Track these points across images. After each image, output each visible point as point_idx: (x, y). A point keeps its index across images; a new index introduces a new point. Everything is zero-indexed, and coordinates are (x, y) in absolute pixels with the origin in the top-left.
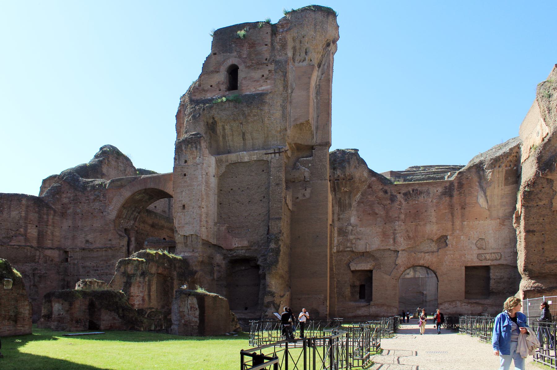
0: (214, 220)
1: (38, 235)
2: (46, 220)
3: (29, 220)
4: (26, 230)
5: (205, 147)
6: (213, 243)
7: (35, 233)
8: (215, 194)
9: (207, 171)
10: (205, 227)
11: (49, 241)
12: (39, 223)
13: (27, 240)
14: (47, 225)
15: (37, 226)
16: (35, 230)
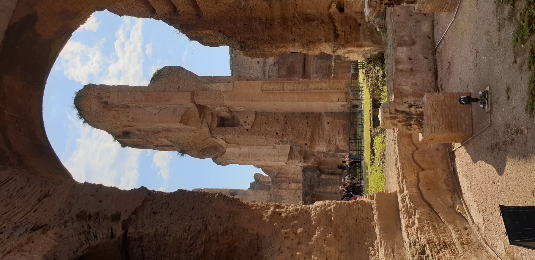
1: (295, 183)
3: (286, 188)
4: (293, 189)
5: (221, 158)
6: (290, 150)
7: (294, 185)
8: (253, 148)
9: (238, 156)
11: (298, 176)
12: (287, 182)
13: (299, 189)
15: (290, 183)
16: (292, 184)
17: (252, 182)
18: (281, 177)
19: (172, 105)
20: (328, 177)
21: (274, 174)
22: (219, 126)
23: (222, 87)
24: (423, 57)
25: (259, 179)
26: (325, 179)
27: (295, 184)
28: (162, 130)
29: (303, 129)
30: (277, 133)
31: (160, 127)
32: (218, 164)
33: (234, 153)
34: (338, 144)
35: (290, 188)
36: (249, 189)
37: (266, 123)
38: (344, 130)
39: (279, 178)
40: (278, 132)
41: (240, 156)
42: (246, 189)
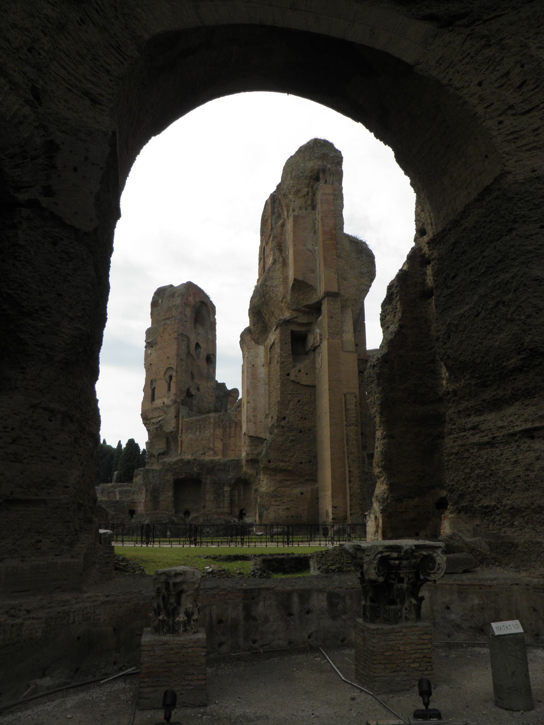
0: (265, 412)
1: (223, 447)
2: (228, 433)
3: (216, 436)
4: (214, 445)
5: (250, 339)
7: (220, 447)
9: (253, 363)
10: (252, 423)
14: (230, 437)
15: (222, 440)
17: (227, 385)
18: (230, 427)
19: (320, 268)
20: (227, 495)
21: (235, 417)
22: (293, 333)
23: (349, 336)
24: (310, 631)
25: (230, 396)
26: (224, 491)
27: (221, 447)
28: (284, 255)
29: (292, 456)
30: (284, 418)
31: (288, 253)
32: (243, 336)
33: (256, 358)
34: (272, 509)
35: (216, 440)
36: (217, 381)
37: (299, 401)
38: (292, 517)
39: (230, 424)
40: (286, 420)
41: (253, 366)
42: (216, 377)
